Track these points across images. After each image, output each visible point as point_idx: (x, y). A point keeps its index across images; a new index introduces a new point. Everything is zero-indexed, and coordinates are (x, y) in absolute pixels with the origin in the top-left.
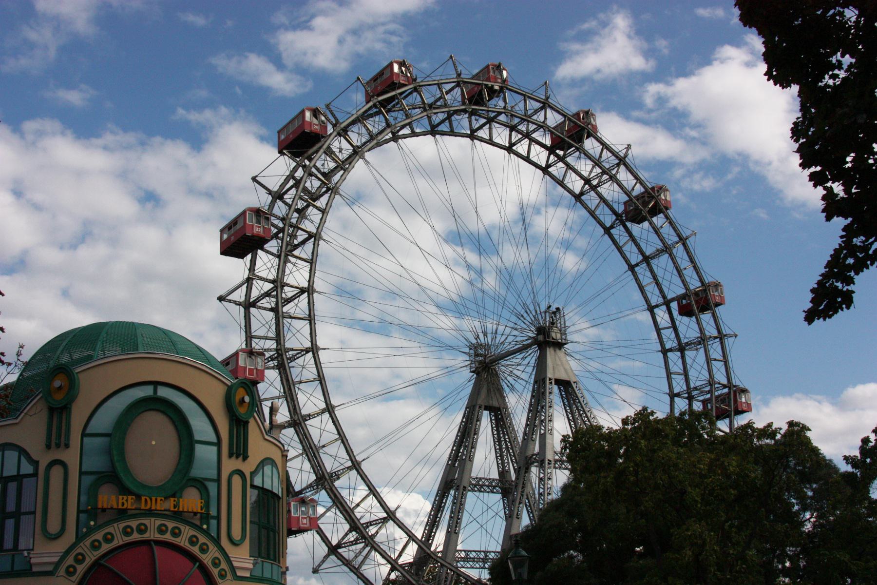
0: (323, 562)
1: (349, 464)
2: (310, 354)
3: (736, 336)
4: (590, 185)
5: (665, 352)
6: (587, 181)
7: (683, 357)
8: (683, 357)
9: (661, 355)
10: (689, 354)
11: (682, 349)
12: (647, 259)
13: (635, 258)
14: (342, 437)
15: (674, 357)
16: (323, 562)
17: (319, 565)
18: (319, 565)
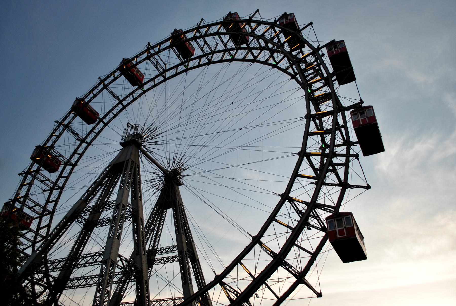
0: (358, 187)
1: (287, 203)
2: (224, 280)
3: (99, 77)
4: (54, 186)
5: (124, 107)
6: (52, 190)
7: (124, 99)
8: (124, 99)
9: (127, 108)
10: (121, 98)
11: (120, 102)
12: (83, 141)
13: (84, 145)
14: (272, 218)
15: (125, 103)
16: (358, 187)
17: (362, 187)
18: (362, 187)
